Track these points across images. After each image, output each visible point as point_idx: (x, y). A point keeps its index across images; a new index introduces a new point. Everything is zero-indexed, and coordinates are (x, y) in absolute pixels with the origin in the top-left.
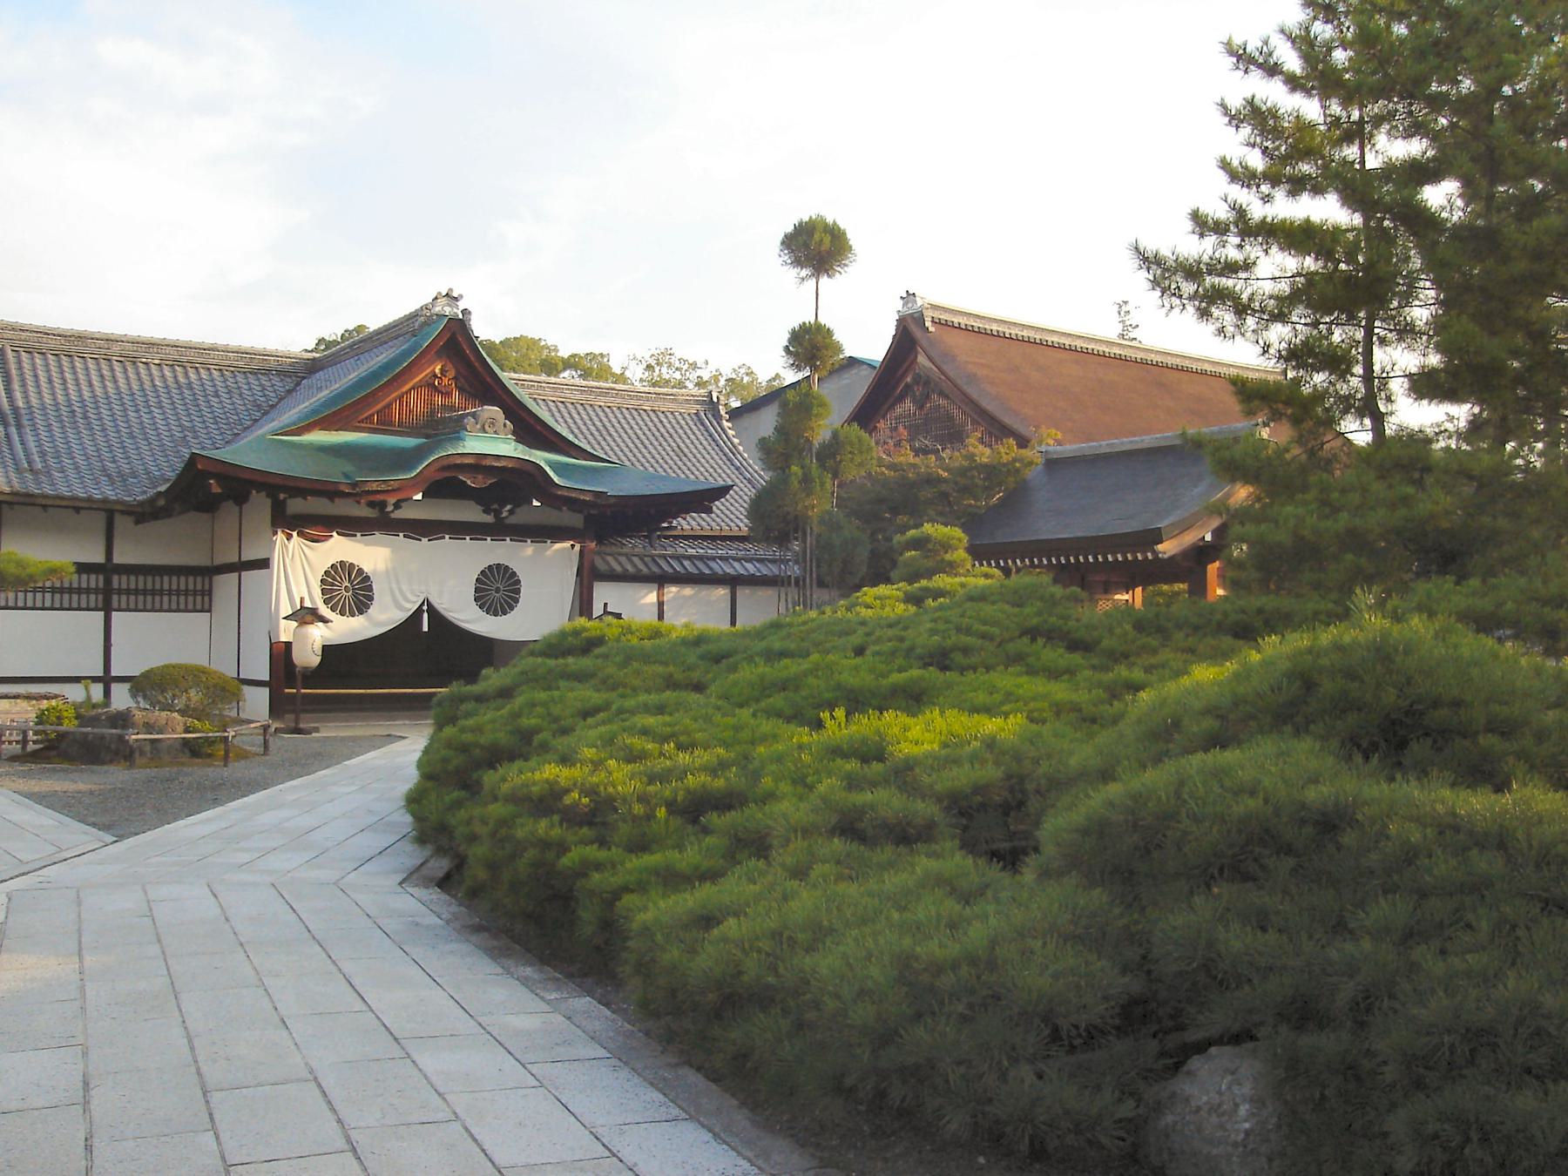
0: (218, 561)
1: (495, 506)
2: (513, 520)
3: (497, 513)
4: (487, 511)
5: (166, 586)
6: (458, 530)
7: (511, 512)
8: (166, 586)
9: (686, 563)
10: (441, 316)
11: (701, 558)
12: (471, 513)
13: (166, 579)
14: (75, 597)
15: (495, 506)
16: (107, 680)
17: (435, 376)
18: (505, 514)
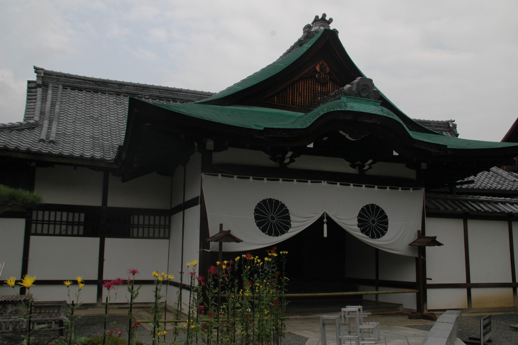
0: (174, 205)
1: (359, 162)
2: (370, 172)
3: (361, 167)
4: (353, 166)
5: (141, 222)
6: (333, 178)
7: (370, 168)
8: (141, 222)
9: (482, 205)
10: (316, 32)
11: (489, 202)
12: (342, 166)
13: (141, 217)
14: (76, 228)
15: (359, 162)
16: (100, 283)
17: (316, 71)
18: (367, 167)
